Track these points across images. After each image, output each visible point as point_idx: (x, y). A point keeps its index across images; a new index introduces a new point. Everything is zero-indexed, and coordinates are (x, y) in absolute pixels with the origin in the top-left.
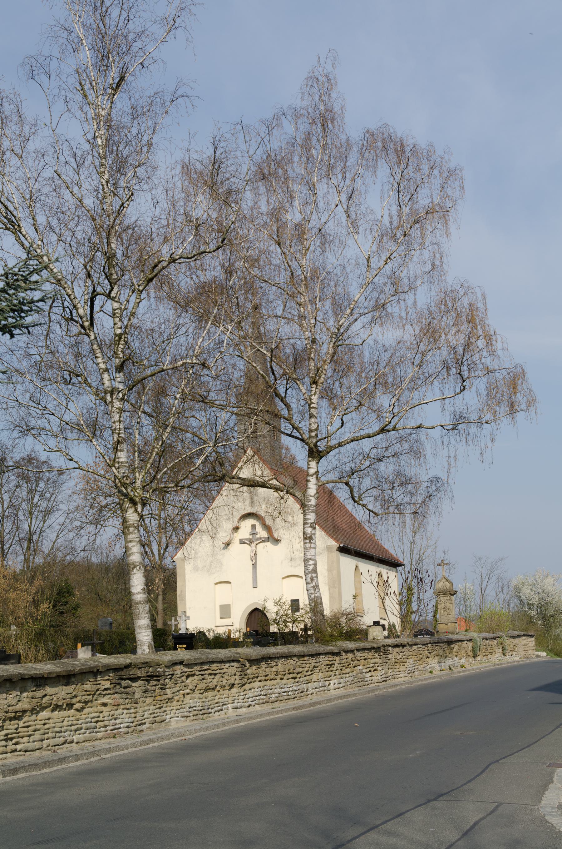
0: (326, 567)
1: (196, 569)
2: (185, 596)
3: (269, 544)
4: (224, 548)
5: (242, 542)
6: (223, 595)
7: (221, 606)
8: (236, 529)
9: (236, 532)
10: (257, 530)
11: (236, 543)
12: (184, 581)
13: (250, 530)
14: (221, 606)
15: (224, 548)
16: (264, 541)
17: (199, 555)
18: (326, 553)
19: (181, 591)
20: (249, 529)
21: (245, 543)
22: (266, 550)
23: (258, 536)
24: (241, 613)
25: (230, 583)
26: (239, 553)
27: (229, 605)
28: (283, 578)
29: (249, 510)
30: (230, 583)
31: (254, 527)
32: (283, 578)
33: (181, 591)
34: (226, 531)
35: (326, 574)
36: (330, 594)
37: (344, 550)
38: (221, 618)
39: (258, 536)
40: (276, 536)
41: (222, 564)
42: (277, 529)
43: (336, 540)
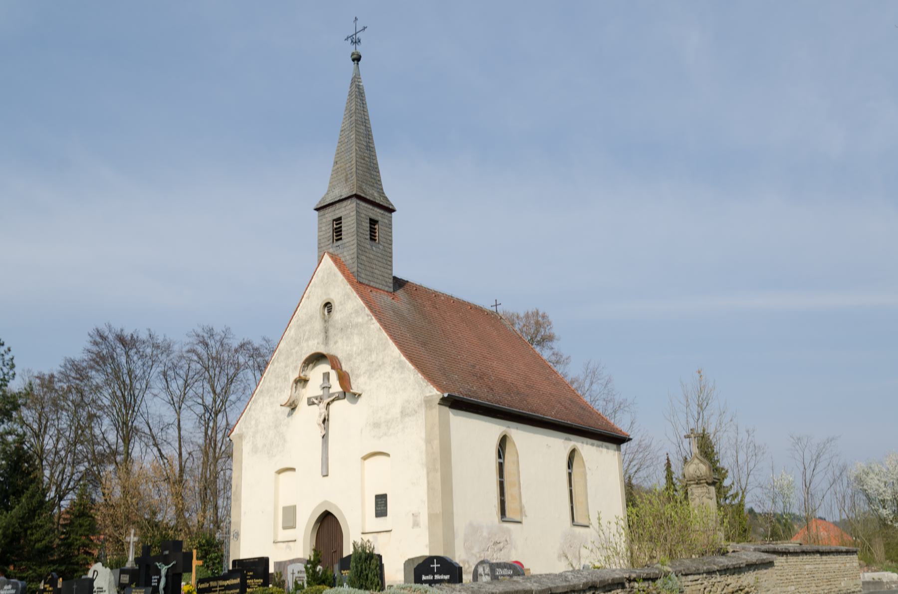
0: (423, 435)
1: (255, 450)
4: (290, 414)
5: (311, 403)
6: (289, 491)
7: (285, 509)
8: (302, 381)
9: (304, 387)
14: (285, 509)
15: (290, 414)
16: (338, 398)
18: (423, 411)
21: (313, 403)
23: (331, 391)
25: (293, 469)
27: (294, 507)
29: (322, 350)
30: (293, 469)
31: (326, 376)
35: (424, 448)
36: (428, 483)
37: (455, 403)
38: (284, 528)
39: (331, 391)
42: (358, 376)
43: (439, 386)
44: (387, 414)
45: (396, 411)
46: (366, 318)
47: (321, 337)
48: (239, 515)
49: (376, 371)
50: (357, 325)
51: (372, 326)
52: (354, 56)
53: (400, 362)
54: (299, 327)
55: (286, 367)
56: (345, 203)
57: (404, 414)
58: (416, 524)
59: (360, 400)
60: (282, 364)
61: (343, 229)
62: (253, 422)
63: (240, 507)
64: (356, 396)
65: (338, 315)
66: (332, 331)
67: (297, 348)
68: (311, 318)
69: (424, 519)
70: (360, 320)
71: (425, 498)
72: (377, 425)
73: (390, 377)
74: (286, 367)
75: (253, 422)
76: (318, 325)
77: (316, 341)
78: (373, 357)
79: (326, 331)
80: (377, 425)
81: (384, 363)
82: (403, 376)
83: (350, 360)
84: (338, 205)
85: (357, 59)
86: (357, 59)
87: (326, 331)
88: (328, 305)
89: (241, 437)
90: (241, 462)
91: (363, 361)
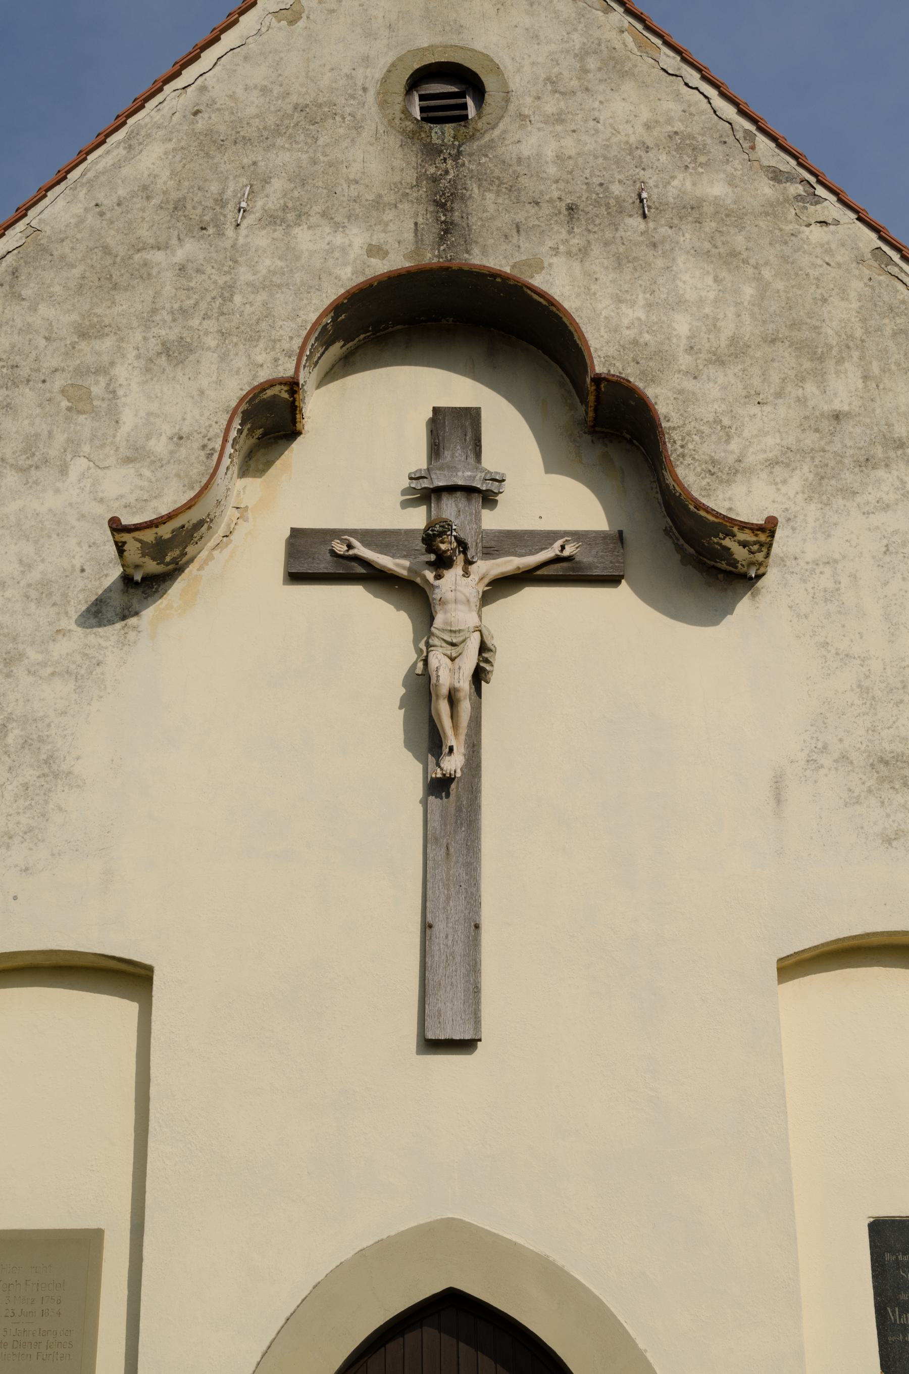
3: (619, 609)
4: (98, 613)
5: (319, 561)
10: (491, 460)
13: (419, 460)
15: (98, 613)
16: (563, 572)
22: (578, 663)
23: (493, 520)
26: (266, 678)
28: (793, 967)
31: (453, 429)
32: (793, 967)
34: (135, 455)
39: (493, 520)
41: (53, 770)
46: (766, 189)
49: (867, 463)
50: (691, 210)
51: (816, 234)
59: (744, 606)
60: (65, 319)
65: (527, 136)
67: (188, 249)
68: (312, 115)
70: (715, 189)
78: (843, 389)
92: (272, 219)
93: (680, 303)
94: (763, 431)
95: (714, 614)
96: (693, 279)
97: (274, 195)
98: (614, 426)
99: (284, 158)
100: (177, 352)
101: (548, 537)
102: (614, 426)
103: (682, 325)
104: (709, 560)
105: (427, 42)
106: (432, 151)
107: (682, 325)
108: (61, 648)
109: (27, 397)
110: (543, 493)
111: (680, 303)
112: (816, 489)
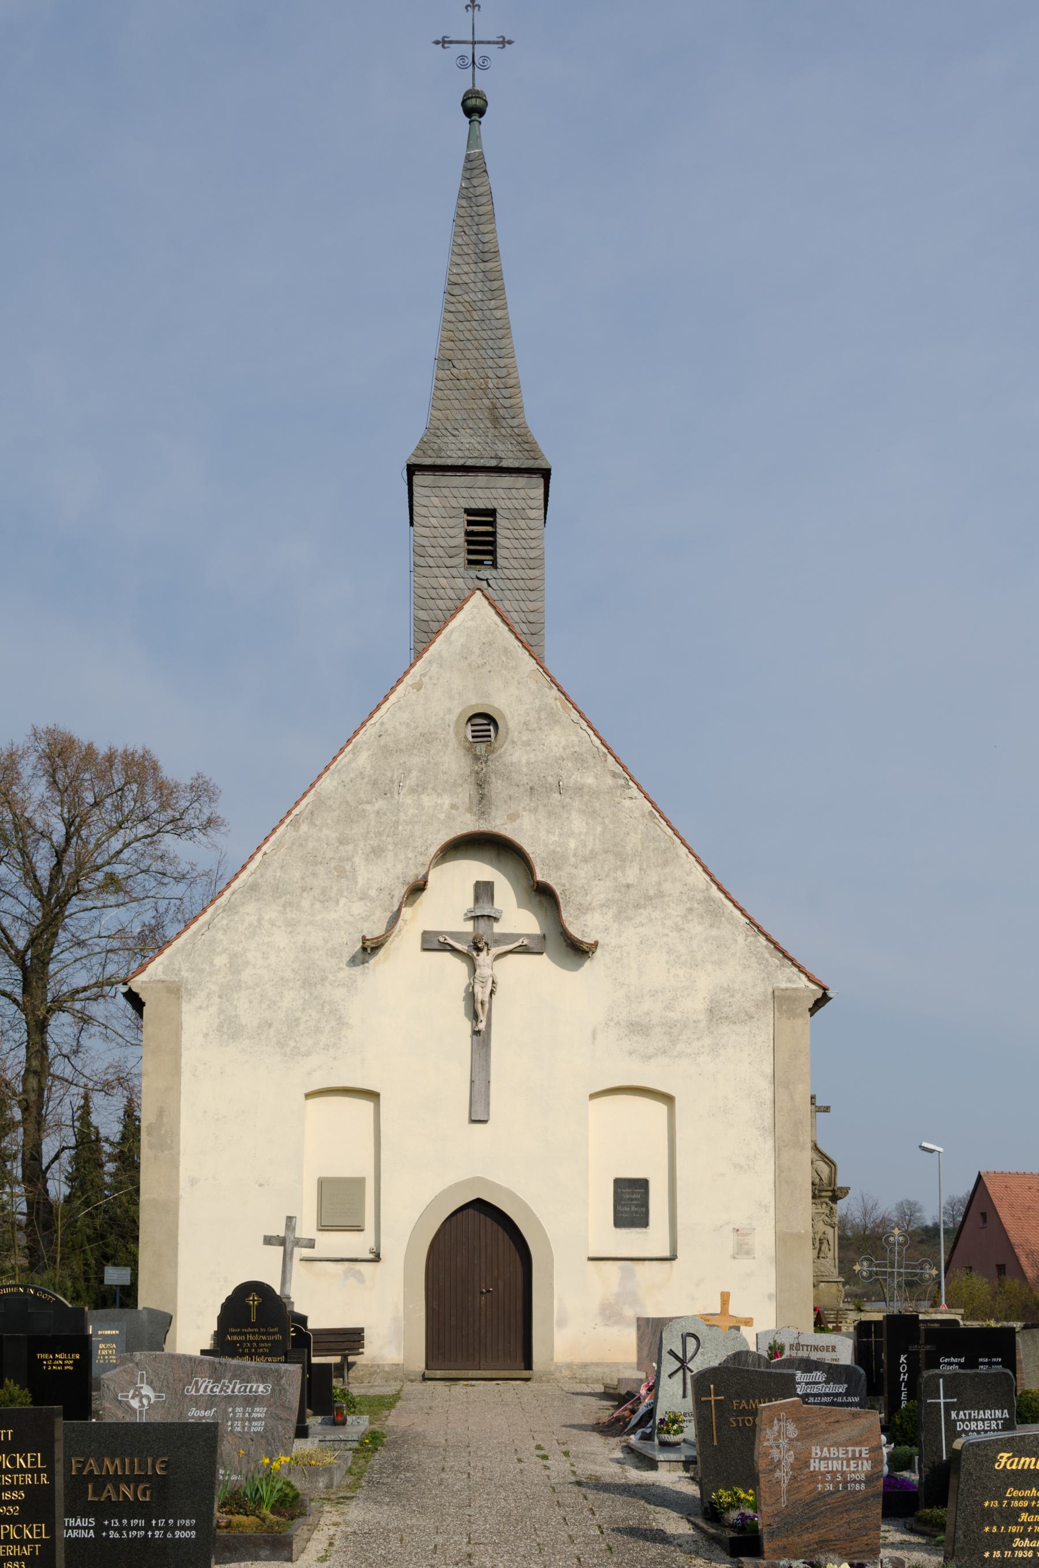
1: (229, 1029)
2: (174, 1133)
3: (542, 965)
4: (353, 961)
5: (434, 943)
10: (498, 903)
11: (406, 941)
12: (176, 1071)
13: (470, 903)
15: (353, 961)
16: (524, 950)
17: (246, 975)
19: (161, 1113)
20: (467, 901)
22: (526, 981)
23: (498, 928)
24: (416, 1216)
28: (593, 1096)
29: (468, 824)
31: (484, 890)
32: (593, 1096)
33: (161, 1113)
34: (364, 897)
36: (779, 1169)
39: (498, 928)
40: (575, 930)
41: (341, 1022)
42: (583, 909)
44: (668, 1008)
45: (695, 1005)
46: (610, 781)
47: (466, 793)
48: (173, 1183)
49: (637, 906)
50: (579, 790)
51: (627, 803)
52: (472, 102)
53: (708, 899)
54: (386, 752)
55: (343, 841)
56: (507, 480)
57: (715, 1014)
58: (743, 1250)
59: (588, 964)
61: (500, 541)
62: (220, 961)
63: (175, 1164)
64: (577, 951)
65: (515, 752)
66: (497, 787)
67: (380, 804)
68: (427, 738)
69: (764, 1240)
70: (590, 780)
71: (769, 1198)
72: (638, 1028)
73: (679, 929)
74: (343, 841)
75: (220, 961)
76: (453, 761)
77: (446, 800)
78: (631, 874)
79: (481, 784)
80: (638, 1028)
81: (660, 894)
82: (714, 932)
83: (558, 868)
84: (482, 479)
85: (474, 108)
86: (474, 108)
87: (481, 784)
88: (484, 724)
89: (175, 991)
90: (176, 1053)
91: (598, 877)
92: (413, 791)
93: (572, 834)
94: (600, 892)
95: (577, 967)
96: (578, 823)
97: (412, 781)
98: (544, 897)
99: (416, 760)
100: (377, 852)
101: (518, 936)
102: (544, 897)
103: (572, 844)
104: (577, 951)
105: (476, 703)
106: (477, 758)
107: (572, 844)
108: (341, 975)
109: (321, 870)
110: (518, 918)
111: (572, 834)
112: (618, 917)
